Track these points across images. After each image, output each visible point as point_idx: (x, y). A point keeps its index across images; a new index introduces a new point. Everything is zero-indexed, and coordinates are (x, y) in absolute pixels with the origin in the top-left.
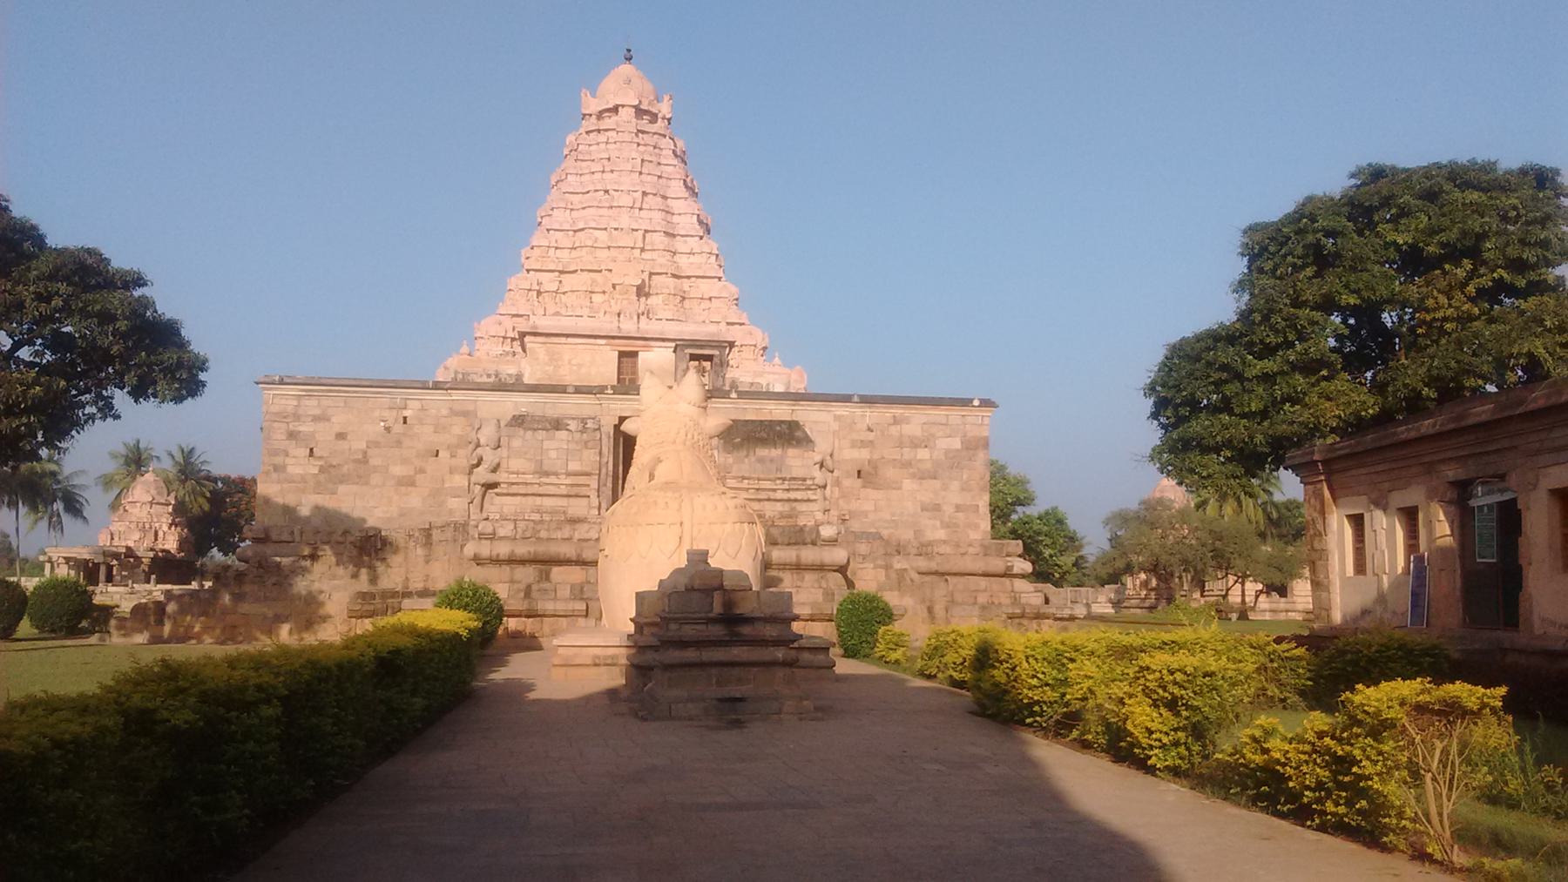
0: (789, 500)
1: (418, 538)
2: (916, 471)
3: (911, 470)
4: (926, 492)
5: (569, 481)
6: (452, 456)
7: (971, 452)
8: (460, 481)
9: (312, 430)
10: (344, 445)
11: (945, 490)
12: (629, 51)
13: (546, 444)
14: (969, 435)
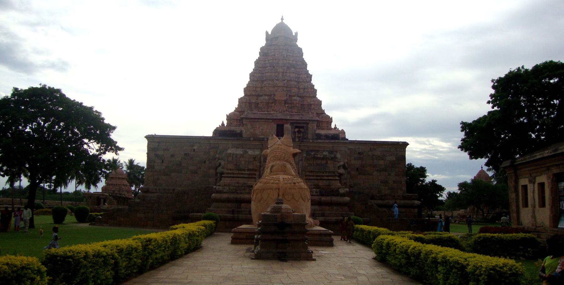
0: (328, 180)
5: (248, 172)
12: (282, 17)
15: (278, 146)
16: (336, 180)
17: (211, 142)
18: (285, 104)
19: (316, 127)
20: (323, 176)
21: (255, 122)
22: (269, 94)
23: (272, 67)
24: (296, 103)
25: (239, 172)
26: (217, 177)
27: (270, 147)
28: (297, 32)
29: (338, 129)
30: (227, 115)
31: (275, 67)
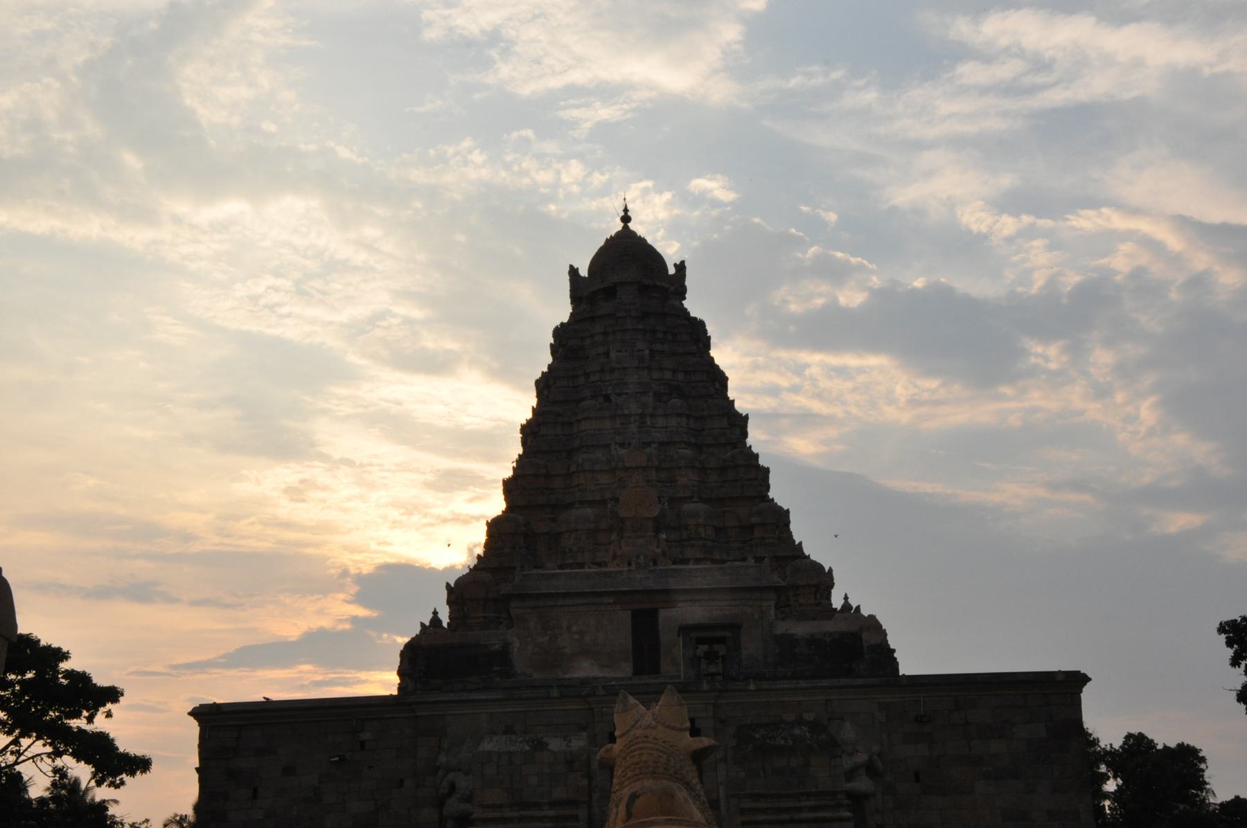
5: (552, 813)
12: (626, 210)
16: (841, 820)
17: (418, 714)
18: (658, 530)
19: (772, 612)
20: (799, 810)
23: (601, 400)
25: (522, 813)
27: (623, 735)
28: (683, 262)
29: (858, 608)
30: (448, 585)
31: (613, 398)
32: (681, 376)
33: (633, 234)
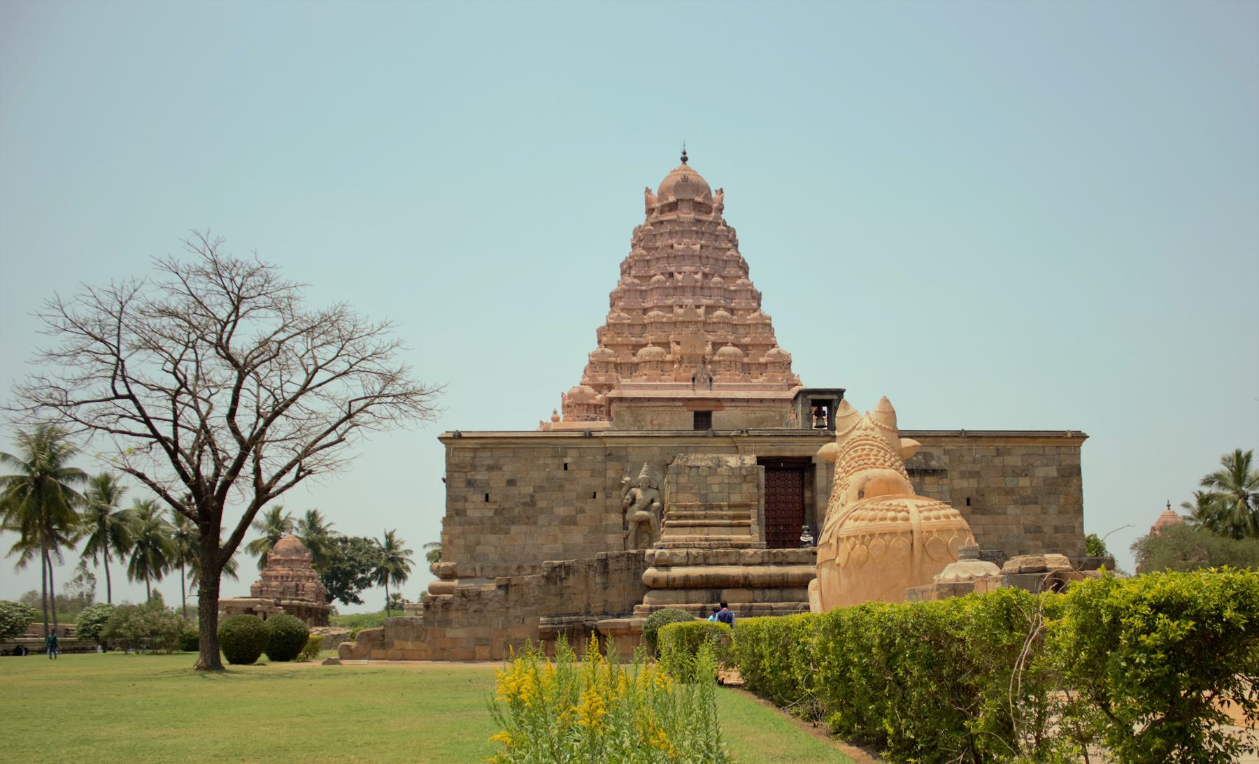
1: (596, 567)
2: (1018, 497)
3: (1014, 497)
4: (1029, 516)
5: (730, 513)
6: (607, 497)
7: (1067, 479)
8: (615, 518)
9: (487, 478)
10: (513, 491)
11: (1045, 513)
12: (684, 153)
13: (710, 480)
14: (1063, 463)
15: (865, 433)
17: (607, 445)
21: (641, 407)
22: (665, 341)
23: (667, 276)
24: (731, 362)
26: (628, 532)
30: (563, 393)
31: (676, 275)
32: (721, 263)
33: (688, 169)
